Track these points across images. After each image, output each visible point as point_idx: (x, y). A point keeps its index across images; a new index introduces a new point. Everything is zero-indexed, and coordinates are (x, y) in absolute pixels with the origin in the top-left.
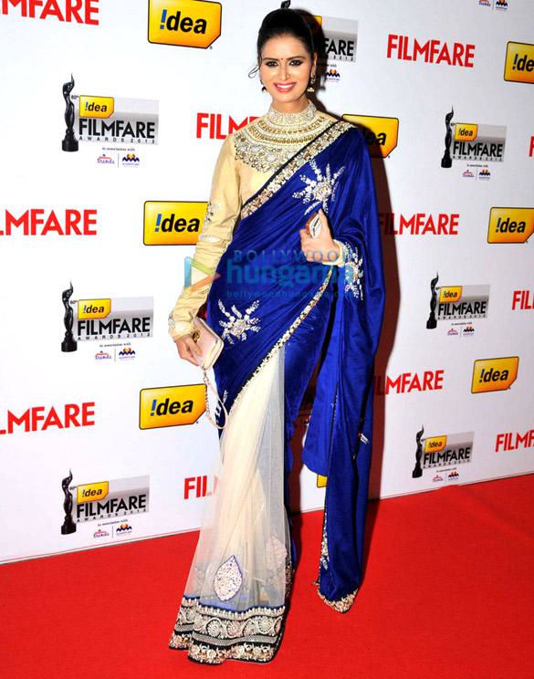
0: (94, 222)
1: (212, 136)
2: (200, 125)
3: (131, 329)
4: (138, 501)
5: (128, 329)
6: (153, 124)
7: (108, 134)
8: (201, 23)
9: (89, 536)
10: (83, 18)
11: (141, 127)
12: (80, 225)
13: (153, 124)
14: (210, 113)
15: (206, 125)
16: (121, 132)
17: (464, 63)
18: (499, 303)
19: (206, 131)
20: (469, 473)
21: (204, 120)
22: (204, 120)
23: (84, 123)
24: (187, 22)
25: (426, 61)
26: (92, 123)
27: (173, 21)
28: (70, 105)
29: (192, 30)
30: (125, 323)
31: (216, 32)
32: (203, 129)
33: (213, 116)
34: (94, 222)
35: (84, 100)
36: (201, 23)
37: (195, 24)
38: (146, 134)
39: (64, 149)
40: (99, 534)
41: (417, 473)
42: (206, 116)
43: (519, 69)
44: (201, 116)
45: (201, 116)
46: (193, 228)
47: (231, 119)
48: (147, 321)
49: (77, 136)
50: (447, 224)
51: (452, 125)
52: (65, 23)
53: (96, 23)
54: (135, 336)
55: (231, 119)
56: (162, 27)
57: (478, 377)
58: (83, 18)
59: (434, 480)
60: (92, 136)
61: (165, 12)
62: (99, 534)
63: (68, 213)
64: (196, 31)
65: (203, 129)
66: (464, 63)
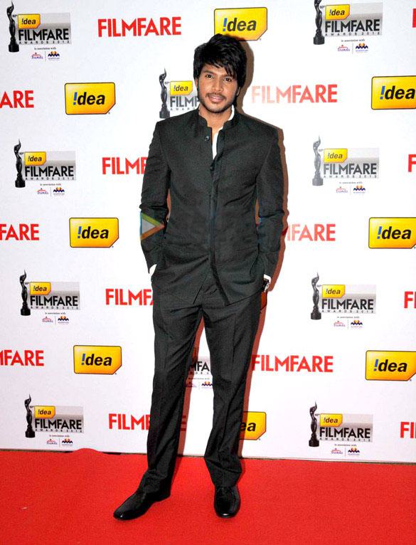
0: (37, 232)
1: (114, 173)
2: (105, 166)
3: (65, 303)
4: (76, 424)
5: (63, 303)
6: (72, 167)
7: (43, 175)
8: (101, 98)
9: (44, 441)
10: (24, 105)
11: (64, 169)
12: (29, 234)
13: (72, 167)
14: (111, 157)
15: (109, 165)
16: (52, 173)
17: (327, 100)
18: (390, 301)
19: (109, 170)
20: (368, 452)
21: (107, 162)
22: (107, 162)
23: (28, 169)
24: (91, 98)
25: (289, 101)
26: (33, 169)
27: (82, 99)
28: (19, 158)
29: (95, 103)
30: (61, 299)
31: (112, 99)
32: (107, 168)
33: (113, 159)
34: (37, 232)
35: (27, 155)
36: (101, 98)
37: (97, 99)
38: (68, 174)
39: (17, 186)
40: (50, 442)
41: (314, 442)
42: (108, 159)
43: (387, 98)
44: (104, 159)
45: (104, 159)
46: (104, 236)
47: (127, 161)
48: (75, 299)
49: (24, 177)
50: (325, 232)
51: (320, 150)
52: (14, 109)
53: (32, 106)
54: (68, 308)
55: (127, 161)
56: (75, 104)
57: (372, 366)
58: (24, 105)
59: (332, 452)
60: (33, 177)
61: (76, 93)
62: (50, 442)
63: (21, 226)
64: (98, 103)
65: (107, 168)
66: (327, 100)
